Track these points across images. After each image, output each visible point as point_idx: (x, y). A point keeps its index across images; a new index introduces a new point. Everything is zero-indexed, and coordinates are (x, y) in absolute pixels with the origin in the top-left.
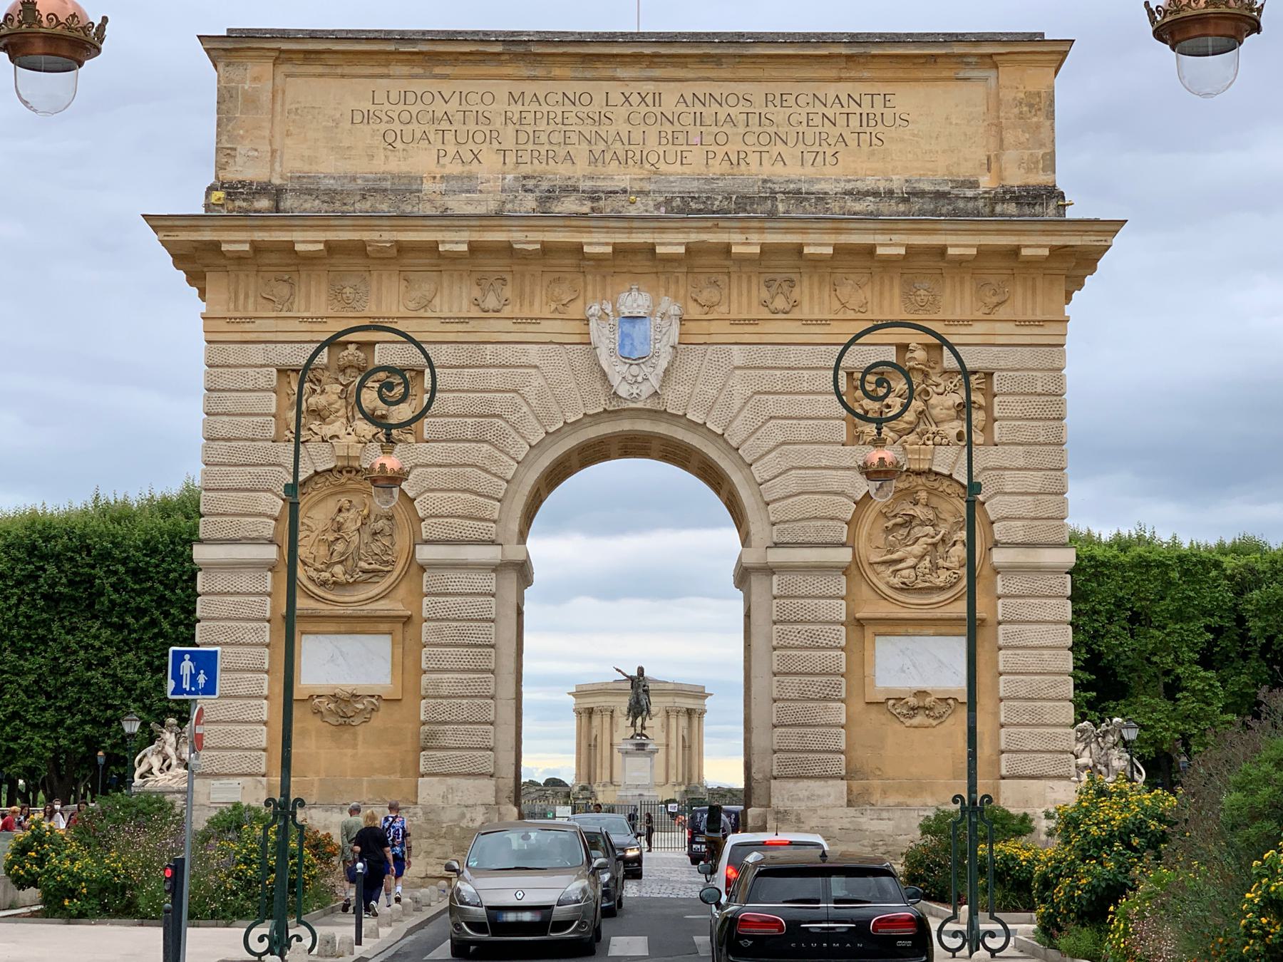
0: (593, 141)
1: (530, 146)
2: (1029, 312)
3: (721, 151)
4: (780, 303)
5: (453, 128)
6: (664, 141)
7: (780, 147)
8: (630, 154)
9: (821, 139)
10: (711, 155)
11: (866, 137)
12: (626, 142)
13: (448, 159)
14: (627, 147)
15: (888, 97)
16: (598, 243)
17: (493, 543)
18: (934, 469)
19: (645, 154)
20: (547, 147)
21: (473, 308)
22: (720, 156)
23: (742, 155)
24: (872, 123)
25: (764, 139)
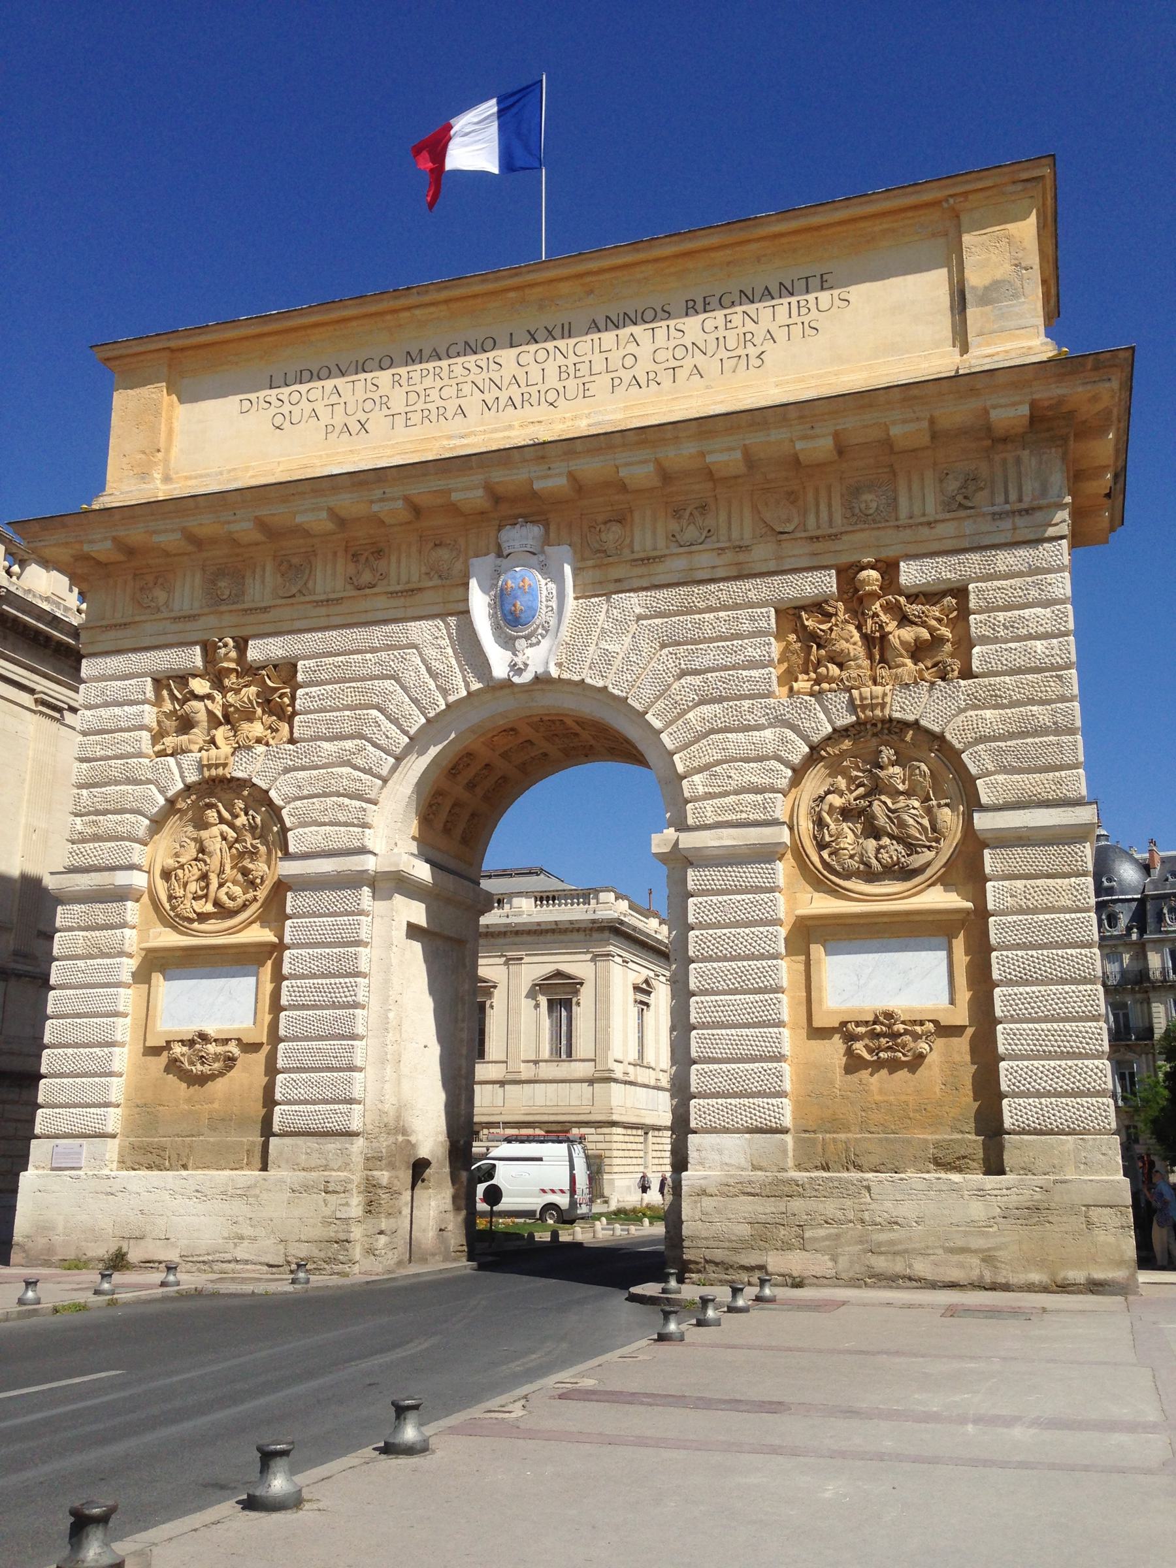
0: (486, 391)
1: (419, 406)
2: (1013, 496)
3: (627, 376)
4: (691, 533)
5: (342, 401)
6: (564, 376)
7: (699, 359)
8: (526, 396)
9: (746, 339)
10: (617, 382)
11: (797, 330)
12: (523, 383)
13: (336, 434)
14: (524, 389)
15: (825, 277)
17: (363, 851)
18: (896, 715)
19: (542, 393)
20: (441, 403)
21: (349, 587)
22: (626, 381)
23: (652, 375)
24: (804, 311)
25: (680, 352)
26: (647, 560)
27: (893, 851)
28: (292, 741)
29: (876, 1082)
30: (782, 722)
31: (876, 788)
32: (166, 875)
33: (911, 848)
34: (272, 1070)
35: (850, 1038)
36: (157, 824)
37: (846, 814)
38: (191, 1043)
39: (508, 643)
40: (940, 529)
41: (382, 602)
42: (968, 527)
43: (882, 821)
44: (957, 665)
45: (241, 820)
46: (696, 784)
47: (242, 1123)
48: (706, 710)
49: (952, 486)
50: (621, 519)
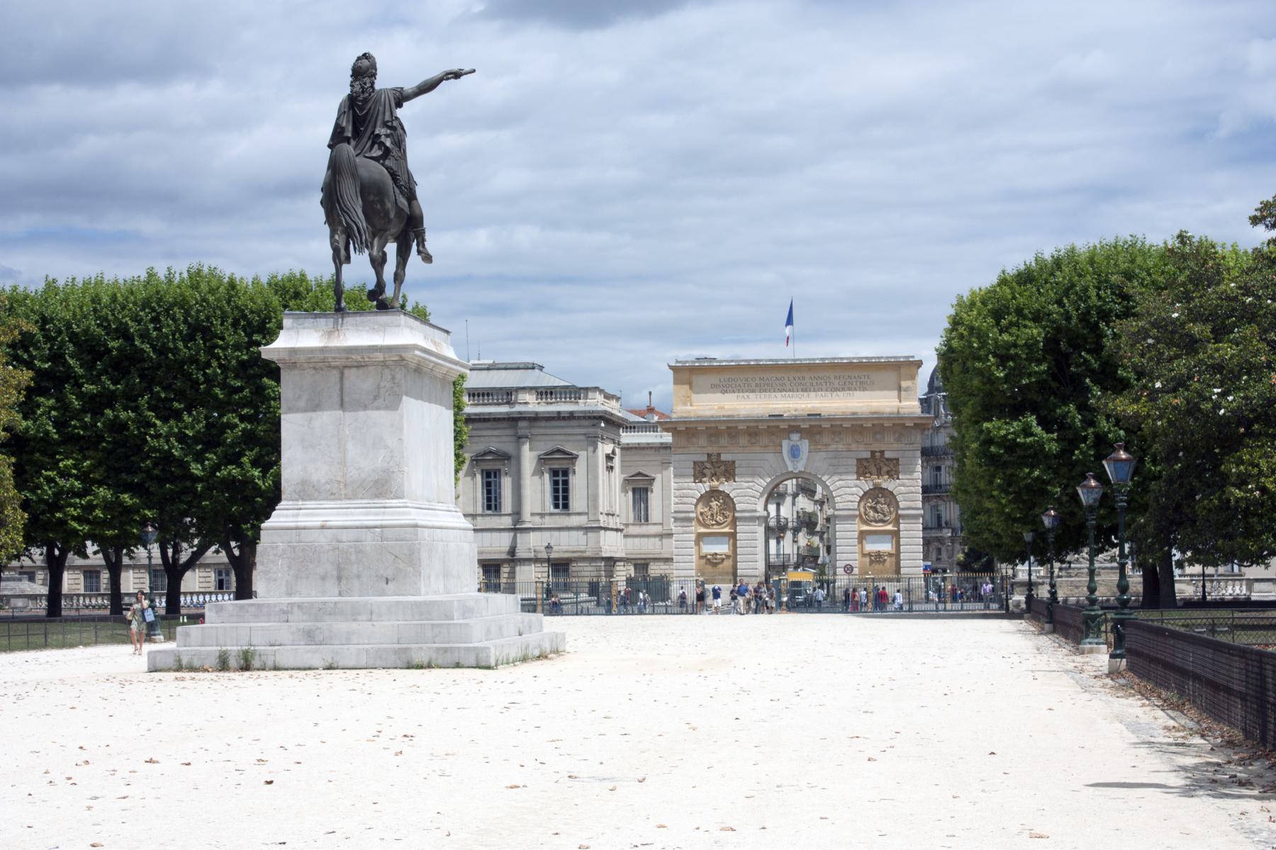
4: (837, 439)
16: (784, 426)
26: (826, 445)
27: (882, 516)
28: (735, 481)
29: (877, 566)
30: (857, 486)
31: (878, 503)
32: (702, 514)
33: (885, 516)
34: (735, 562)
35: (871, 556)
36: (699, 500)
37: (871, 507)
38: (713, 555)
39: (793, 462)
40: (894, 445)
41: (758, 448)
42: (900, 446)
43: (879, 510)
44: (896, 476)
45: (721, 501)
46: (837, 499)
47: (727, 574)
48: (840, 482)
49: (897, 435)
50: (820, 433)
